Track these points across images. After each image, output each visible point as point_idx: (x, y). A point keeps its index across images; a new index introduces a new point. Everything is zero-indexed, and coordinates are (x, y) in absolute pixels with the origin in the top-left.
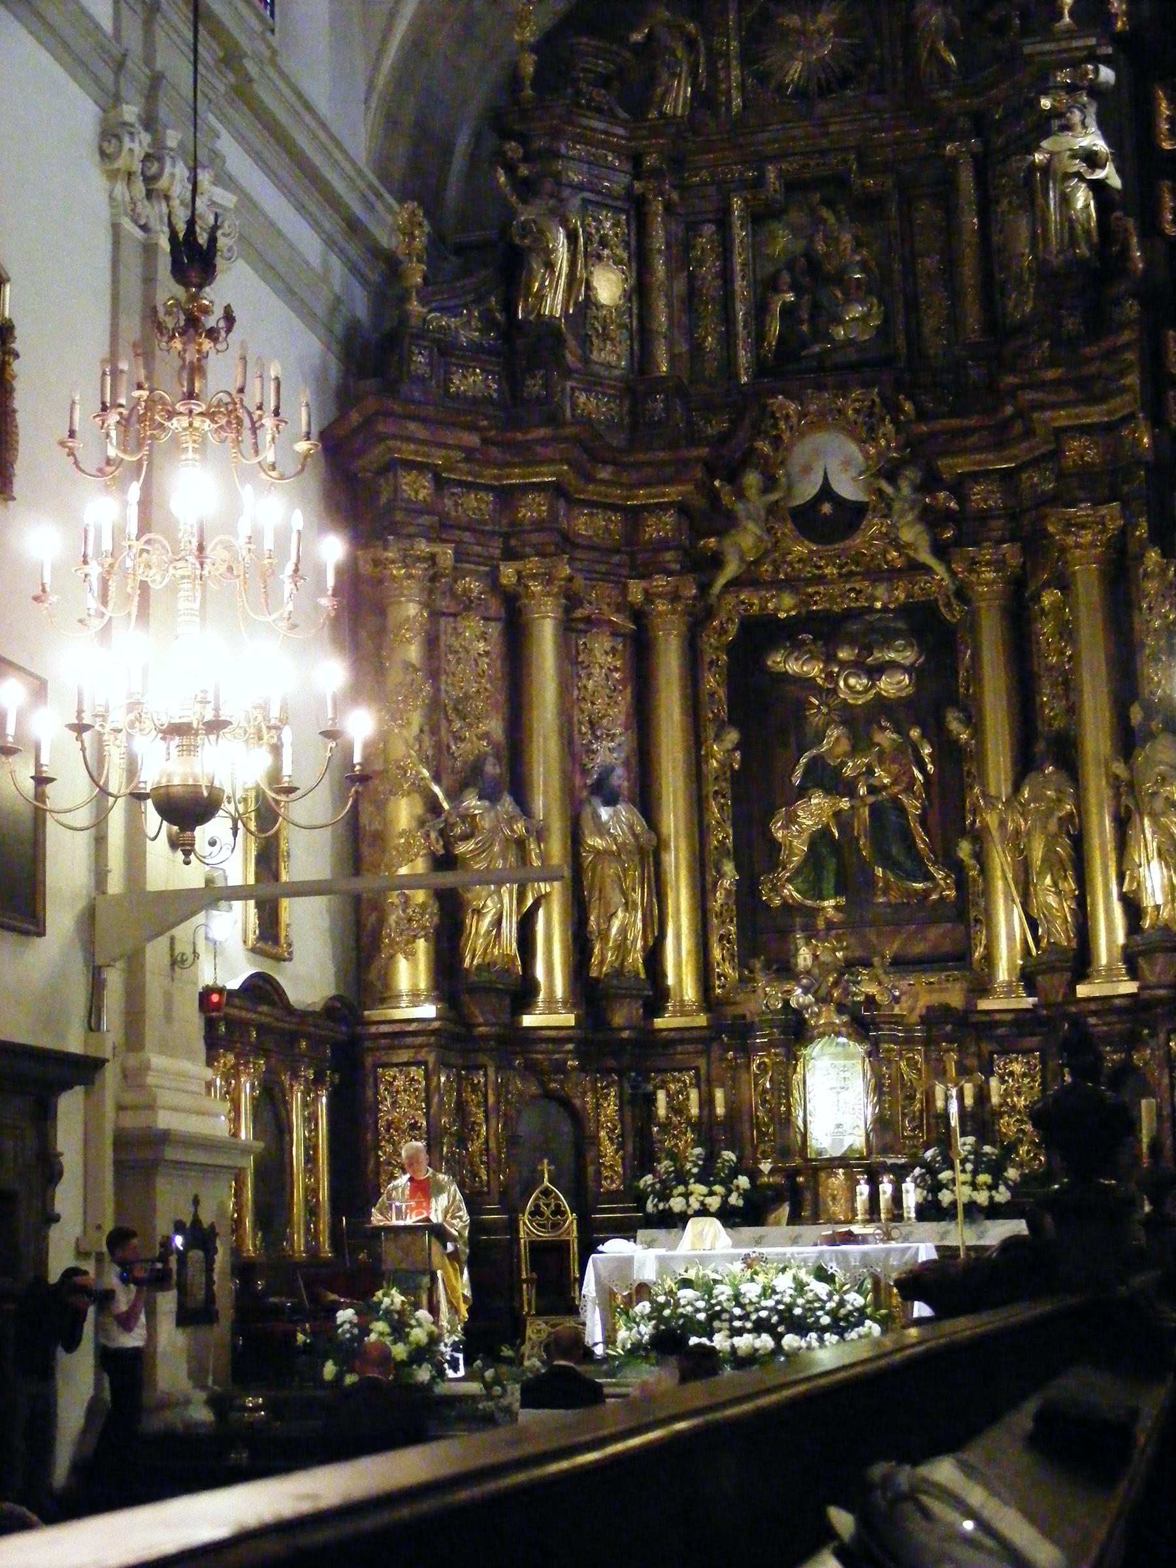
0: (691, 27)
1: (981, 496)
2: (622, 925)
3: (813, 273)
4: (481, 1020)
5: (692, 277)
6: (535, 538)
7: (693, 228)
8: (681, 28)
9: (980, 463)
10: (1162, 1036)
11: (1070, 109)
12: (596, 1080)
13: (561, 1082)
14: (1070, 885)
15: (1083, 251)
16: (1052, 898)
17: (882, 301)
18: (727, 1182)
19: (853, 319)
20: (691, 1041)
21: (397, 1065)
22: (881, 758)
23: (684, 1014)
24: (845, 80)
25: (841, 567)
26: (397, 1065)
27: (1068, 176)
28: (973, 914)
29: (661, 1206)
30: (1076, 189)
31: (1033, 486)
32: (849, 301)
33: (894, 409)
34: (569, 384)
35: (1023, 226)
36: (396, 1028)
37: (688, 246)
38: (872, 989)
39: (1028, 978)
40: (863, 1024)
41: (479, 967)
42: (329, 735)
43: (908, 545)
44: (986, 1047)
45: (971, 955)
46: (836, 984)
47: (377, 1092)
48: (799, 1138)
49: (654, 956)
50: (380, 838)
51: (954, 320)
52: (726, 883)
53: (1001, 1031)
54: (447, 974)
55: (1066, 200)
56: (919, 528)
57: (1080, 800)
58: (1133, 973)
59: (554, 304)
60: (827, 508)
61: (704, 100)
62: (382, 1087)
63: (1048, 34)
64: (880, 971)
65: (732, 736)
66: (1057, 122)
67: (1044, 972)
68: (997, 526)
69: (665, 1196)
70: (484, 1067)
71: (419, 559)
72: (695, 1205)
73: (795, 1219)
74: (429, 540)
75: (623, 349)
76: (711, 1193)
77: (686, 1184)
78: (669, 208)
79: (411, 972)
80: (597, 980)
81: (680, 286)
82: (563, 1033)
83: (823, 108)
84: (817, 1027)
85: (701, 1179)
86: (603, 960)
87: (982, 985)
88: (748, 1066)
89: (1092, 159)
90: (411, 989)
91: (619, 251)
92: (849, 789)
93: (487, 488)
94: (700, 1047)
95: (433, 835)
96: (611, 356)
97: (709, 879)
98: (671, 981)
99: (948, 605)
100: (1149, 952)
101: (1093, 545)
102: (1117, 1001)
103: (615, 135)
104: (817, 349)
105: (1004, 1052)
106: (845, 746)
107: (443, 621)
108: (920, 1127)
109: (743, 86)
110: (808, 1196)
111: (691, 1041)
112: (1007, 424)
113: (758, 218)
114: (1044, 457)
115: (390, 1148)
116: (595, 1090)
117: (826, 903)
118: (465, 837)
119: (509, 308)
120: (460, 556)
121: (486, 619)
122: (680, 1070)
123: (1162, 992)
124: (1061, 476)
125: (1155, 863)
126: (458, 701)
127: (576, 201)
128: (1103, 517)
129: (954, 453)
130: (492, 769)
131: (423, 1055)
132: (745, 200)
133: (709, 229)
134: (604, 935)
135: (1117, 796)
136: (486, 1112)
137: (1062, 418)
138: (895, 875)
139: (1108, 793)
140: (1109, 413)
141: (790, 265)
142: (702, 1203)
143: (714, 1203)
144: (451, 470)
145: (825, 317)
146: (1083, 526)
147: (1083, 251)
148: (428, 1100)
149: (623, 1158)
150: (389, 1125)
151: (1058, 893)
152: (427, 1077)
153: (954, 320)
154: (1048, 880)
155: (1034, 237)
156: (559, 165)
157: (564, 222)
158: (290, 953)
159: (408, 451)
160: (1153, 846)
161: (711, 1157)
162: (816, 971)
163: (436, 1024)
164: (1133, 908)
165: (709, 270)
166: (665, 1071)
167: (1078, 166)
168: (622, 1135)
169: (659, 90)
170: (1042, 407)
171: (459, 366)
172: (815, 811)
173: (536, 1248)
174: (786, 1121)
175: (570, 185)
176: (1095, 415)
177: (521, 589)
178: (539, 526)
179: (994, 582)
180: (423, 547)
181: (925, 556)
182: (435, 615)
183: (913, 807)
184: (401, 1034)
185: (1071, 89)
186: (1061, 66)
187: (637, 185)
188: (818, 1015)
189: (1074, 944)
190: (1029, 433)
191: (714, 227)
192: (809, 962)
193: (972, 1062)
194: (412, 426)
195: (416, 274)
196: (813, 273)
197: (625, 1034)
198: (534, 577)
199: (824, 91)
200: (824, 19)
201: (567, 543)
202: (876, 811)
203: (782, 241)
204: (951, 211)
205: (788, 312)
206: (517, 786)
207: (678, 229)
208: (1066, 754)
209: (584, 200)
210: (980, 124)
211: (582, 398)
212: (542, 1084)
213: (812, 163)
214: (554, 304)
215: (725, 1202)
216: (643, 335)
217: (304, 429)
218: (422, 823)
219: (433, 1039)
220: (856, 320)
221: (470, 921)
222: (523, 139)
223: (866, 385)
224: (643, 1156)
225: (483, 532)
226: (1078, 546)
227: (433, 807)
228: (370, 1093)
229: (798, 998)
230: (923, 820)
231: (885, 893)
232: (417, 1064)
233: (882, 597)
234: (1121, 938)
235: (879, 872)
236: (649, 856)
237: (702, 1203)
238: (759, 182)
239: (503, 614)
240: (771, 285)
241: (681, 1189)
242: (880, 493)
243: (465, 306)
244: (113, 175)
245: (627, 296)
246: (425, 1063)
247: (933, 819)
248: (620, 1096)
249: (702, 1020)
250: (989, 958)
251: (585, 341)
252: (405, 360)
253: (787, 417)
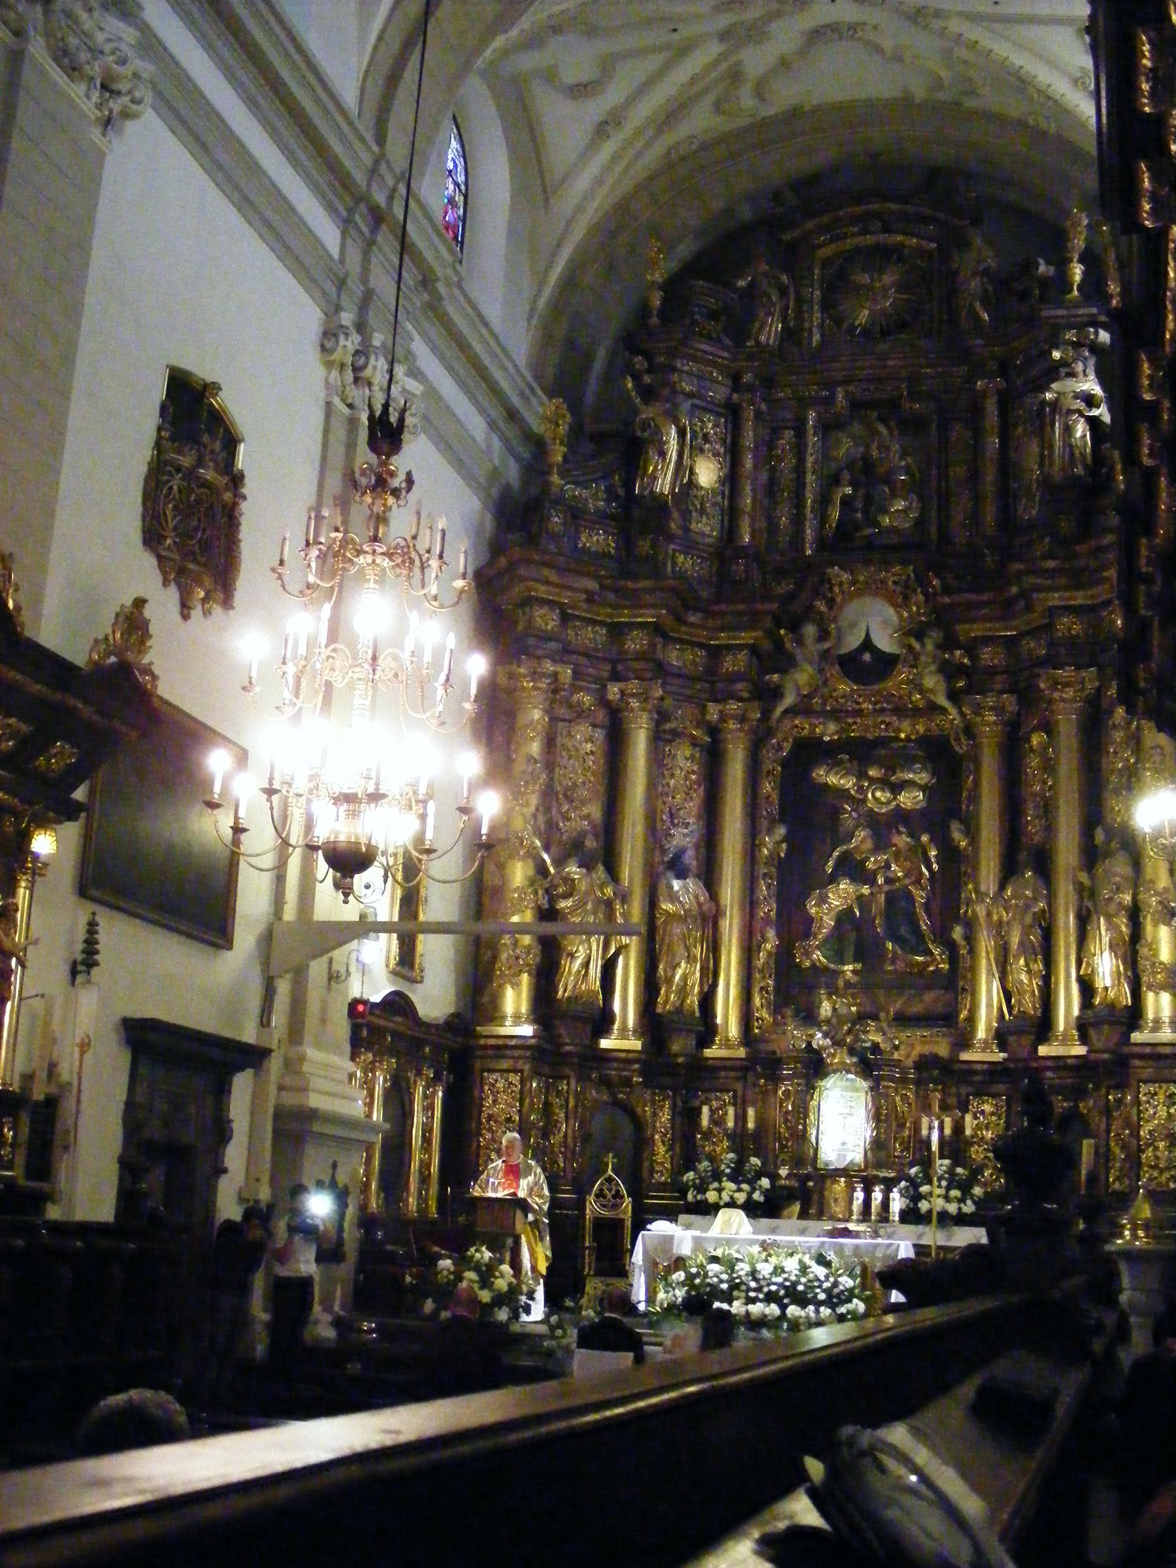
0: (784, 278)
1: (988, 656)
2: (684, 973)
3: (867, 473)
4: (568, 1041)
5: (773, 469)
6: (636, 665)
7: (775, 433)
8: (777, 278)
9: (990, 629)
10: (1104, 1091)
11: (1075, 360)
12: (654, 1094)
13: (627, 1094)
14: (1039, 966)
15: (1079, 470)
16: (1024, 976)
17: (921, 498)
18: (752, 1182)
19: (897, 511)
20: (733, 1069)
21: (501, 1071)
22: (897, 856)
23: (729, 1047)
24: (902, 326)
25: (875, 704)
26: (501, 1071)
27: (1070, 412)
28: (961, 983)
29: (699, 1197)
30: (1076, 422)
31: (1030, 650)
32: (894, 495)
33: (923, 583)
34: (672, 547)
35: (1034, 448)
36: (501, 1042)
37: (771, 445)
38: (877, 1038)
39: (1001, 1037)
40: (868, 1065)
41: (569, 998)
42: (464, 810)
43: (931, 691)
44: (964, 1090)
45: (957, 1016)
46: (849, 1032)
47: (482, 1091)
48: (811, 1151)
49: (707, 1001)
50: (499, 892)
51: (975, 516)
52: (769, 946)
53: (977, 1078)
54: (544, 1004)
55: (1068, 430)
56: (940, 677)
57: (1051, 899)
58: (1084, 1039)
59: (664, 484)
60: (867, 657)
61: (791, 335)
62: (486, 1087)
63: (1059, 305)
64: (884, 1025)
65: (781, 831)
66: (1063, 370)
67: (1015, 1033)
68: (999, 681)
69: (702, 1189)
70: (568, 1077)
71: (544, 675)
72: (726, 1197)
73: (804, 1215)
74: (554, 661)
75: (715, 522)
76: (739, 1190)
77: (720, 1182)
78: (758, 415)
80: (660, 1015)
81: (764, 476)
82: (631, 1055)
83: (882, 347)
84: (831, 1064)
85: (733, 1178)
86: (667, 1000)
87: (964, 1040)
88: (776, 1092)
89: (1090, 400)
90: (515, 1014)
91: (717, 447)
92: (867, 878)
93: (602, 624)
94: (739, 1074)
95: (540, 892)
96: (706, 527)
97: (754, 943)
98: (719, 1021)
99: (958, 739)
100: (1097, 1024)
101: (1074, 700)
102: (1069, 1061)
103: (719, 357)
104: (868, 531)
105: (978, 1094)
106: (869, 844)
107: (561, 724)
108: (907, 1149)
109: (821, 326)
110: (815, 1197)
111: (733, 1069)
112: (1011, 601)
113: (827, 428)
114: (1038, 629)
115: (488, 1136)
116: (653, 1102)
117: (846, 968)
118: (565, 896)
119: (629, 484)
120: (577, 674)
121: (594, 725)
122: (721, 1091)
123: (1106, 1056)
124: (1052, 645)
125: (1106, 954)
126: (567, 789)
127: (686, 405)
128: (1084, 678)
129: (972, 621)
130: (590, 843)
131: (520, 1064)
132: (818, 413)
133: (789, 434)
134: (669, 981)
135: (1081, 898)
136: (567, 1113)
137: (1055, 599)
138: (902, 949)
139: (1073, 897)
140: (1092, 597)
141: (850, 466)
142: (731, 1197)
143: (741, 1198)
144: (573, 608)
145: (873, 507)
146: (1067, 685)
147: (1079, 470)
148: (521, 1101)
149: (672, 1158)
150: (490, 1117)
151: (1029, 972)
152: (522, 1082)
153: (975, 516)
154: (1022, 962)
155: (1042, 456)
156: (676, 377)
157: (676, 422)
158: (422, 977)
159: (542, 591)
160: (1106, 939)
161: (741, 1162)
162: (834, 1021)
163: (533, 1041)
164: (1087, 988)
165: (787, 465)
166: (710, 1091)
167: (1079, 404)
168: (672, 1139)
169: (757, 325)
170: (1039, 589)
171: (586, 527)
172: (841, 895)
173: (598, 1222)
174: (803, 1137)
175: (683, 393)
176: (1080, 598)
177: (623, 705)
178: (640, 656)
179: (995, 723)
180: (549, 666)
181: (942, 700)
182: (554, 719)
183: (920, 896)
184: (504, 1048)
185: (1077, 345)
186: (1070, 327)
187: (735, 396)
188: (834, 1056)
189: (1039, 1014)
190: (1029, 609)
191: (792, 433)
192: (829, 1013)
193: (952, 1101)
194: (546, 572)
195: (558, 454)
196: (867, 473)
197: (681, 1060)
198: (633, 695)
199: (885, 333)
200: (888, 279)
201: (661, 670)
202: (891, 898)
203: (845, 447)
204: (978, 432)
205: (846, 502)
206: (609, 858)
207: (764, 432)
208: (1043, 864)
209: (694, 406)
210: (1004, 367)
211: (681, 558)
212: (613, 1094)
213: (872, 388)
214: (664, 484)
215: (750, 1194)
216: (732, 514)
217: (461, 570)
218: (532, 883)
219: (528, 1054)
220: (899, 512)
221: (565, 962)
222: (648, 355)
223: (904, 563)
224: (687, 1157)
225: (597, 658)
226: (1063, 700)
227: (542, 870)
228: (476, 1093)
229: (819, 1040)
230: (927, 907)
231: (893, 963)
232: (515, 1071)
233: (906, 730)
234: (1076, 1012)
235: (890, 945)
236: (710, 921)
237: (731, 1197)
238: (829, 401)
239: (607, 723)
240: (836, 481)
241: (716, 1185)
242: (910, 648)
243: (595, 481)
244: (329, 365)
245: (722, 481)
246: (522, 1071)
247: (936, 909)
248: (673, 1107)
249: (741, 1053)
250: (972, 1020)
251: (686, 515)
252: (544, 519)
253: (841, 584)
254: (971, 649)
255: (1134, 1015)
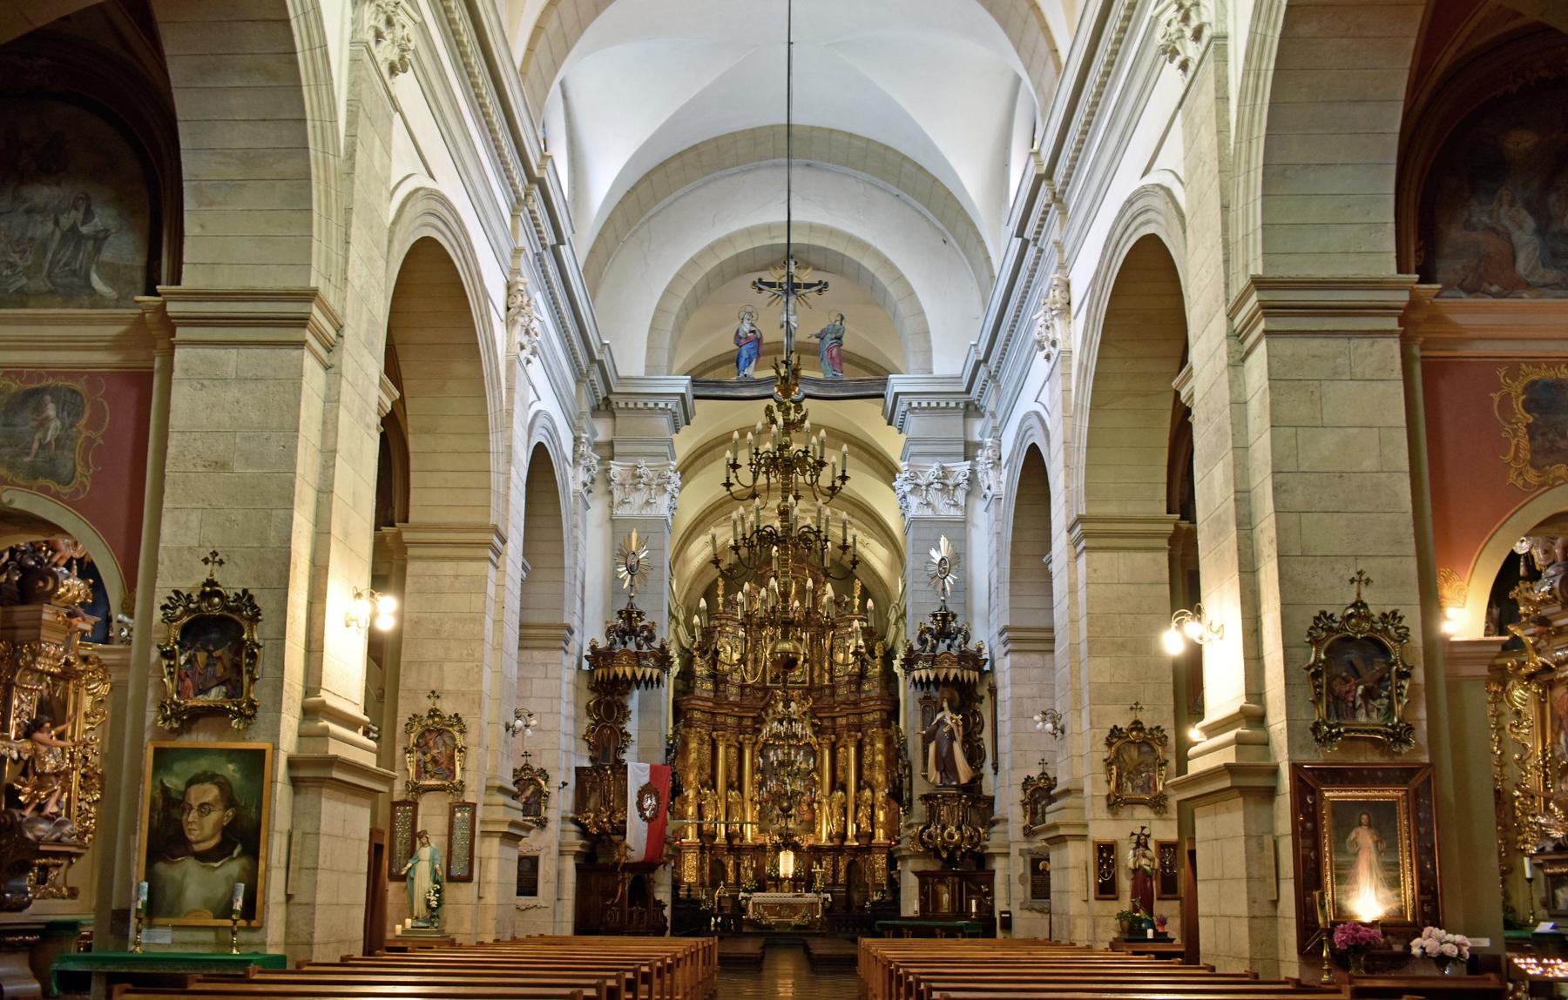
1: (827, 723)
39: (830, 838)
79: (691, 832)
153: (821, 676)
164: (858, 827)
206: (714, 786)
208: (844, 788)
254: (821, 719)
255: (872, 836)
